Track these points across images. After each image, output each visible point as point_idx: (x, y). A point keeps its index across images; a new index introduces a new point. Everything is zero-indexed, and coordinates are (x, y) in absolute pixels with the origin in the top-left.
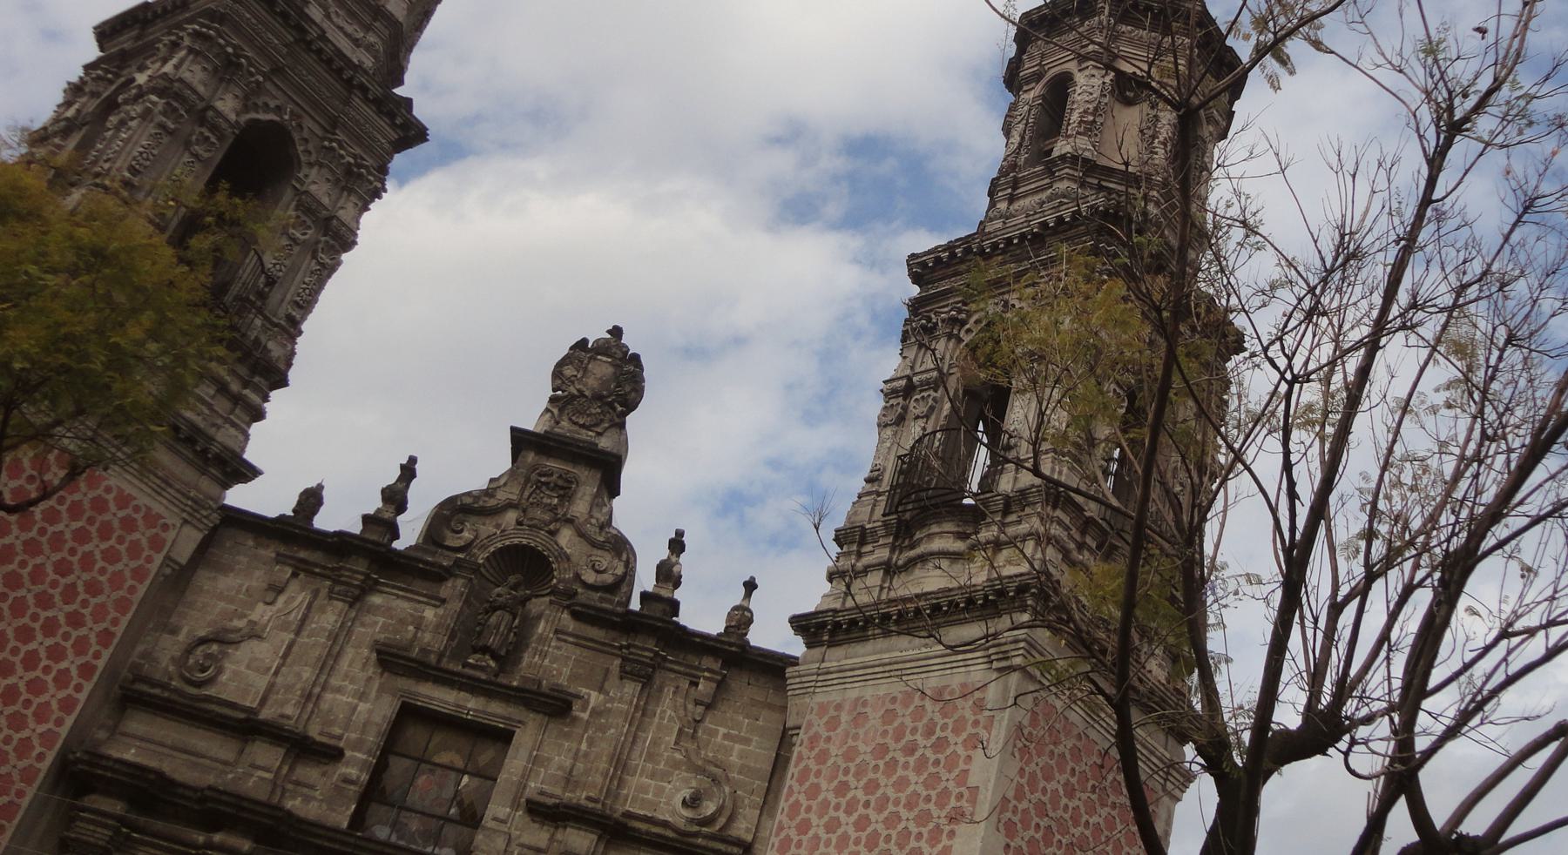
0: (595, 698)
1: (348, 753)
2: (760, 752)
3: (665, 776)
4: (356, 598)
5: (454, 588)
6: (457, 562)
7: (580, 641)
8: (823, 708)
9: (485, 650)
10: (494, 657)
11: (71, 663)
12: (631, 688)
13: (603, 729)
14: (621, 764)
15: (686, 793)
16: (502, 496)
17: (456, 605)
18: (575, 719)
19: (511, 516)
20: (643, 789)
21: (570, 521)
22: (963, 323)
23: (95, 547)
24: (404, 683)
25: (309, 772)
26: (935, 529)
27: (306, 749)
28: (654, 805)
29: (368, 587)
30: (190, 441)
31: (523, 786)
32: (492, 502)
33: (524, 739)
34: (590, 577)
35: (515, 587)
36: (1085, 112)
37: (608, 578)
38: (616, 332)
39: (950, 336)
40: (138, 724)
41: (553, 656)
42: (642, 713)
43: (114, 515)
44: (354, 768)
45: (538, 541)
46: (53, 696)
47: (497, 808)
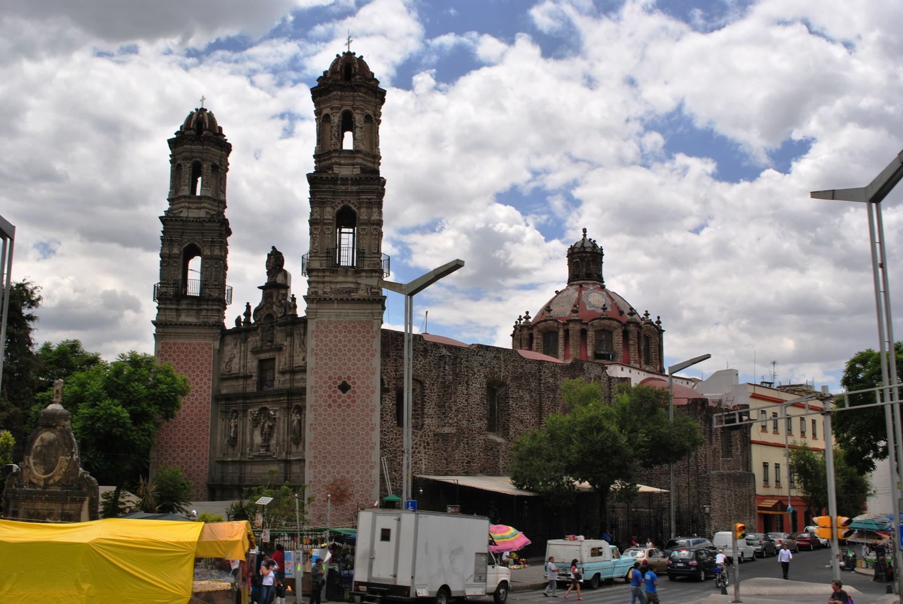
4: (245, 341)
11: (205, 380)
14: (291, 356)
23: (198, 356)
25: (249, 382)
27: (247, 377)
38: (273, 248)
40: (225, 384)
43: (198, 348)
46: (205, 387)
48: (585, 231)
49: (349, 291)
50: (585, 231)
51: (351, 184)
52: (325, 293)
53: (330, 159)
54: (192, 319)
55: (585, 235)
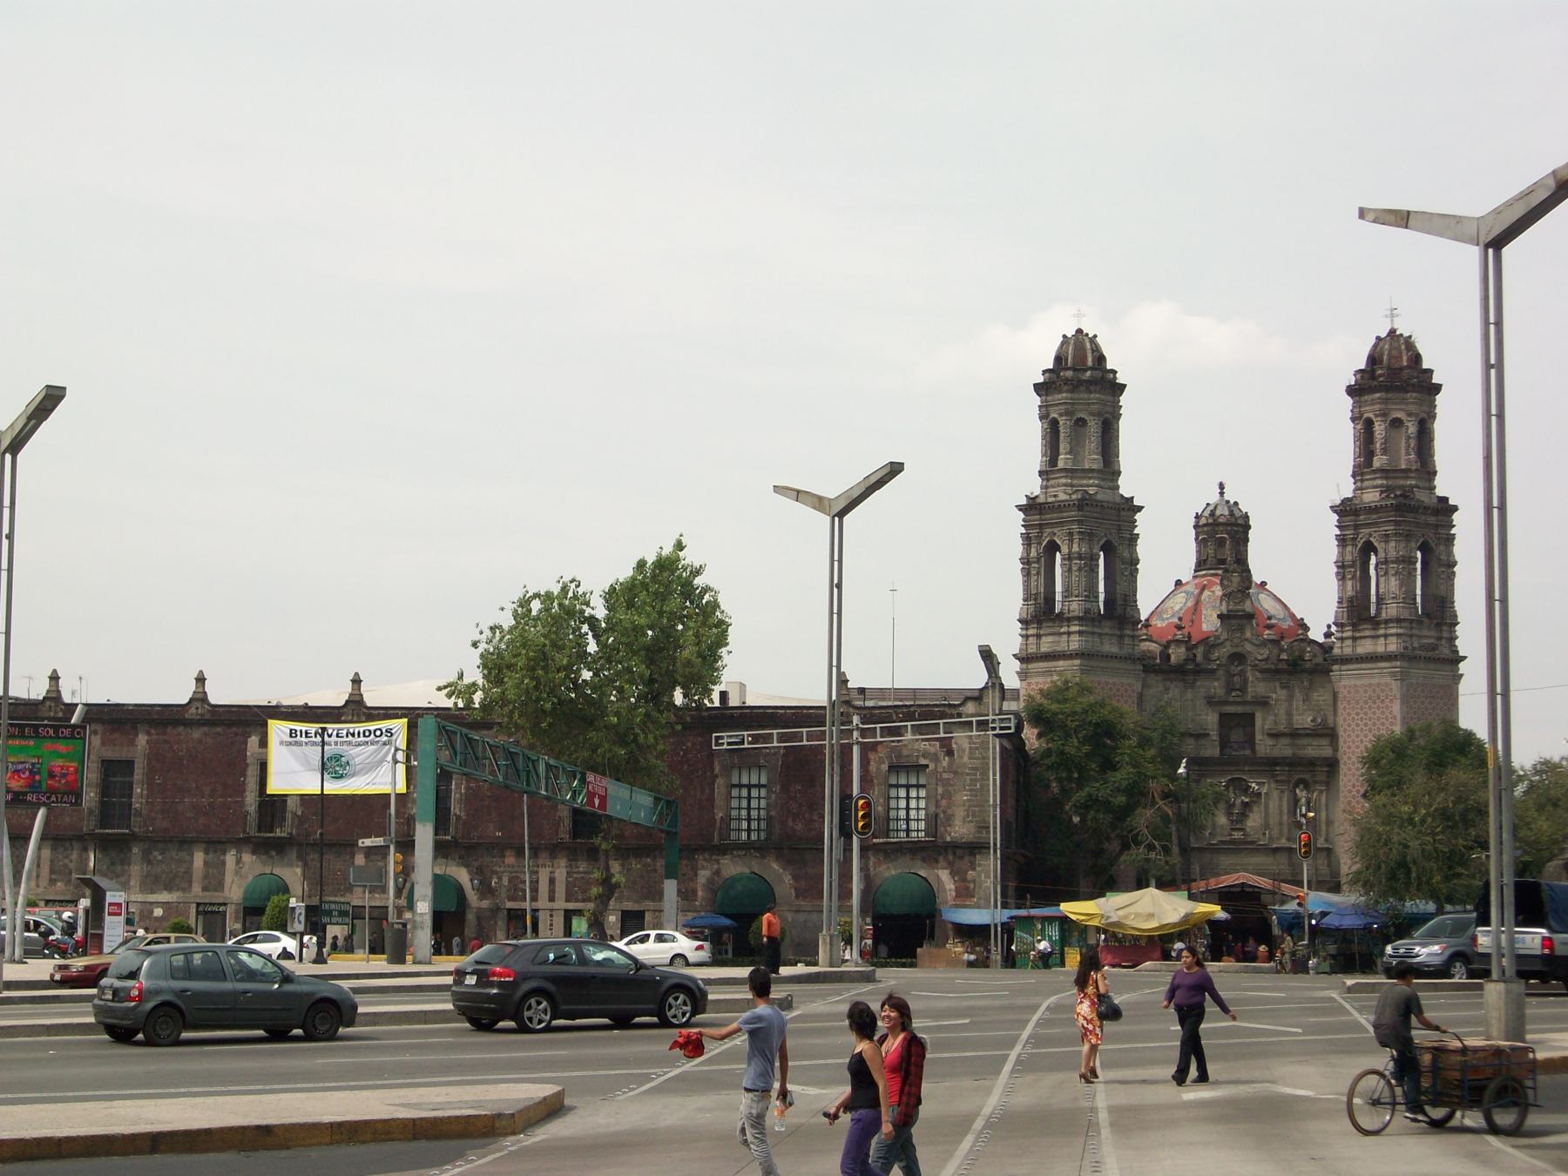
2: (1328, 697)
7: (1264, 680)
14: (1289, 714)
19: (1228, 644)
25: (1203, 741)
41: (1257, 687)
42: (1291, 698)
44: (1214, 735)
45: (1239, 650)
47: (1258, 737)
48: (1221, 486)
49: (1434, 648)
50: (1221, 486)
54: (1114, 649)
55: (1222, 494)
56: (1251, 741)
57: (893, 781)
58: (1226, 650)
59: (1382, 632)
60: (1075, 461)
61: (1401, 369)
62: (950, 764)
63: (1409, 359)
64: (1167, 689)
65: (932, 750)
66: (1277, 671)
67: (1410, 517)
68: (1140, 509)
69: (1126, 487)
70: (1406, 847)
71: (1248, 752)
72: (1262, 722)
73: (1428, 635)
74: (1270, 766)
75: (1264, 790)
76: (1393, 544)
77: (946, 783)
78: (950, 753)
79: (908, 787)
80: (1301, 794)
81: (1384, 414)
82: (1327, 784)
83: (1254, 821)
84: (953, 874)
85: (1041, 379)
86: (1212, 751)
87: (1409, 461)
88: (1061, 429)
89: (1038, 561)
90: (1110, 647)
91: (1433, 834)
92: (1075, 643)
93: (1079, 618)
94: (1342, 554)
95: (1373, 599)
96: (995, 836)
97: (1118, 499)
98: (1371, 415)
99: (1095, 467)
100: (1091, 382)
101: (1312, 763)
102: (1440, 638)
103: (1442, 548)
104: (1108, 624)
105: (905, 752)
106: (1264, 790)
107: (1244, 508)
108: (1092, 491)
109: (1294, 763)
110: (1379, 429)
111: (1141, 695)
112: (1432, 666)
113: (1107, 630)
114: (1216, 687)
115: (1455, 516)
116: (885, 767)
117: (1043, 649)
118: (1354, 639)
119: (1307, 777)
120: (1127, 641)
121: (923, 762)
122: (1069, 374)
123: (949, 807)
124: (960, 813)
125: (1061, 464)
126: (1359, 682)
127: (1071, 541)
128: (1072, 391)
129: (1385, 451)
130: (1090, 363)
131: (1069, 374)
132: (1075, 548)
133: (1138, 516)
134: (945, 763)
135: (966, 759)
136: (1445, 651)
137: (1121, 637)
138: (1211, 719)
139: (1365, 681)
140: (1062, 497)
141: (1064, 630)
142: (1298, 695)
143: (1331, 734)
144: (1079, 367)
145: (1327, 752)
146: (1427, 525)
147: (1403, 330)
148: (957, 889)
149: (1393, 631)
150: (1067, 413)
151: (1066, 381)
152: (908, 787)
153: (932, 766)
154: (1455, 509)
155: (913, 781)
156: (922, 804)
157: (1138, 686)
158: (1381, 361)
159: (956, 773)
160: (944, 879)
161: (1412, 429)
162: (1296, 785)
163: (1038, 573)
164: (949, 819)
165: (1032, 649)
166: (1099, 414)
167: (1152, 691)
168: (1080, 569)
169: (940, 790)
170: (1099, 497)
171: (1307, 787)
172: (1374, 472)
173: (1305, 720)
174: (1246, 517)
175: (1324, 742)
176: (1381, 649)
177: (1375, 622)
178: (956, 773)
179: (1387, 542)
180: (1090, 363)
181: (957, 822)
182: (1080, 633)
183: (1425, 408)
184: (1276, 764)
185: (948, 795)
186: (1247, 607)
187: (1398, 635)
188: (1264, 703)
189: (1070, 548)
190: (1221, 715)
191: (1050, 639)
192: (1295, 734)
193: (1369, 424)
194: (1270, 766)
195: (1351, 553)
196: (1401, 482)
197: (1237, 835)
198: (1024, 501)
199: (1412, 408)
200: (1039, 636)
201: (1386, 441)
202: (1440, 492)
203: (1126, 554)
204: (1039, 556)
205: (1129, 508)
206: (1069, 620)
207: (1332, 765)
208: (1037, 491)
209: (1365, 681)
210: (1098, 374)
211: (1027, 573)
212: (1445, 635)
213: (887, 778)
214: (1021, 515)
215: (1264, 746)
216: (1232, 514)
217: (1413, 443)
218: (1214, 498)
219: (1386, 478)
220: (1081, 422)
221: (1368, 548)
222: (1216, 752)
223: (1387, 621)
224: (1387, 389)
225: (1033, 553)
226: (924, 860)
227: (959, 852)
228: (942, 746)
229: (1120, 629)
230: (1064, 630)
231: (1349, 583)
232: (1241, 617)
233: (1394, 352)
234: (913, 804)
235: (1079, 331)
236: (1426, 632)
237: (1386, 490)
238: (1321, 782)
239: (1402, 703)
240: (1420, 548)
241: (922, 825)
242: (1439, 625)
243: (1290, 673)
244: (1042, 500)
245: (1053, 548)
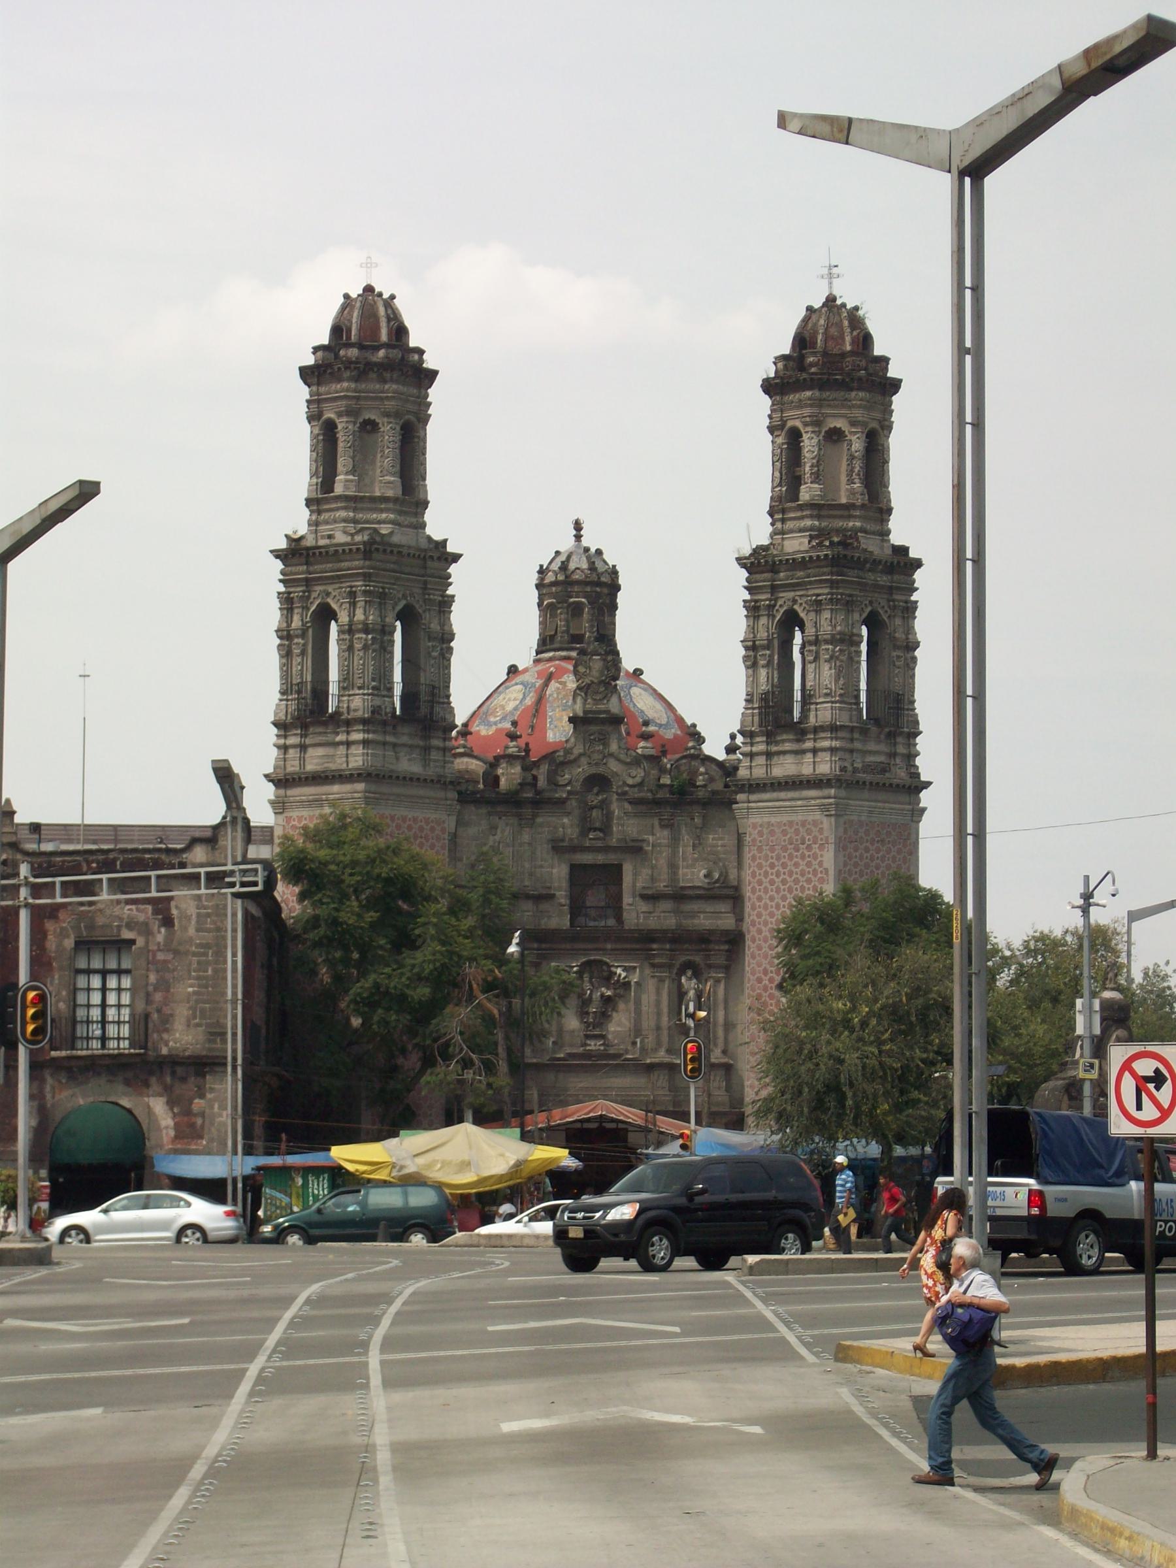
0: (651, 838)
1: (558, 893)
2: (730, 841)
3: (693, 866)
5: (573, 803)
6: (569, 793)
7: (636, 815)
8: (754, 826)
9: (595, 829)
10: (600, 830)
12: (666, 833)
13: (660, 852)
14: (673, 867)
15: (704, 872)
16: (576, 752)
17: (576, 812)
18: (646, 853)
19: (584, 760)
20: (685, 875)
21: (611, 755)
22: (774, 606)
24: (567, 856)
25: (545, 906)
26: (785, 737)
28: (692, 880)
29: (535, 816)
30: (439, 781)
31: (634, 886)
32: (572, 757)
33: (628, 869)
34: (630, 781)
35: (597, 794)
36: (812, 466)
37: (638, 780)
39: (768, 615)
41: (626, 825)
42: (675, 841)
44: (562, 896)
45: (601, 770)
47: (627, 899)
48: (578, 526)
50: (578, 526)
51: (882, 572)
52: (855, 770)
53: (850, 517)
54: (416, 768)
55: (578, 537)
56: (615, 905)
57: (82, 964)
58: (581, 771)
59: (809, 745)
60: (359, 484)
61: (843, 355)
62: (169, 939)
63: (854, 342)
64: (493, 828)
65: (141, 918)
66: (657, 803)
67: (852, 576)
68: (456, 558)
69: (438, 523)
70: (841, 1062)
71: (611, 922)
72: (633, 877)
73: (875, 750)
74: (643, 942)
75: (635, 979)
76: (826, 615)
77: (162, 967)
78: (168, 922)
79: (104, 973)
80: (689, 984)
81: (817, 423)
82: (727, 969)
83: (619, 1024)
84: (171, 1103)
85: (310, 360)
86: (559, 920)
87: (852, 493)
88: (341, 436)
89: (303, 635)
90: (408, 765)
91: (880, 1043)
92: (357, 759)
93: (364, 721)
94: (752, 629)
95: (797, 695)
96: (234, 1047)
97: (423, 544)
98: (798, 423)
99: (390, 493)
100: (386, 367)
101: (704, 939)
102: (893, 755)
103: (898, 621)
104: (406, 729)
105: (100, 921)
106: (635, 979)
107: (610, 558)
108: (385, 529)
109: (678, 938)
110: (810, 444)
111: (454, 837)
112: (882, 796)
113: (405, 739)
114: (566, 825)
115: (918, 575)
116: (69, 943)
117: (310, 767)
118: (769, 755)
119: (697, 959)
120: (435, 755)
121: (127, 935)
122: (353, 353)
123: (166, 1001)
124: (182, 1012)
125: (339, 489)
126: (773, 820)
127: (353, 604)
128: (357, 380)
129: (817, 477)
130: (384, 337)
131: (353, 353)
132: (359, 616)
133: (453, 569)
134: (160, 938)
135: (191, 931)
136: (900, 774)
137: (427, 749)
138: (558, 873)
139: (785, 818)
140: (341, 538)
141: (341, 737)
142: (686, 838)
143: (733, 896)
144: (368, 343)
145: (727, 922)
146: (876, 587)
147: (848, 298)
148: (177, 1126)
149: (826, 744)
150: (348, 413)
151: (348, 364)
152: (104, 973)
153: (140, 942)
154: (918, 564)
155: (112, 964)
156: (126, 999)
157: (450, 823)
158: (813, 344)
159: (176, 953)
160: (158, 1111)
161: (857, 444)
162: (682, 972)
163: (303, 653)
164: (166, 1020)
165: (293, 767)
166: (397, 415)
167: (472, 831)
168: (365, 648)
169: (152, 978)
170: (395, 539)
171: (697, 974)
172: (801, 508)
173: (695, 875)
174: (614, 572)
175: (724, 907)
176: (807, 770)
177: (800, 731)
178: (176, 953)
179: (818, 612)
180: (384, 337)
181: (179, 1025)
182: (365, 743)
183: (878, 415)
184: (653, 940)
185: (164, 986)
186: (613, 706)
187: (832, 750)
188: (635, 849)
189: (352, 615)
190: (573, 867)
191: (320, 751)
192: (680, 896)
193: (794, 437)
194: (643, 942)
195: (766, 628)
196: (840, 524)
197: (594, 1045)
198: (283, 544)
199: (858, 414)
200: (303, 748)
201: (819, 461)
202: (896, 539)
203: (435, 626)
204: (305, 627)
205: (440, 557)
206: (348, 723)
207: (734, 941)
208: (303, 529)
209: (785, 818)
210: (396, 354)
211: (286, 653)
212: (901, 749)
213: (72, 959)
214: (279, 565)
215: (636, 913)
216: (592, 567)
217: (858, 466)
218: (566, 543)
219: (819, 517)
220: (370, 427)
221: (791, 621)
222: (566, 923)
223: (816, 730)
224: (821, 384)
225: (296, 623)
226: (127, 1083)
227: (180, 1070)
228: (156, 912)
229: (426, 737)
230: (341, 737)
231: (763, 673)
232: (603, 722)
233: (833, 331)
234: (112, 999)
235: (369, 289)
236: (872, 746)
237: (819, 535)
238: (717, 967)
239: (837, 851)
240: (865, 622)
241: (125, 1031)
242: (891, 736)
243: (676, 805)
244: (310, 542)
245: (325, 615)
